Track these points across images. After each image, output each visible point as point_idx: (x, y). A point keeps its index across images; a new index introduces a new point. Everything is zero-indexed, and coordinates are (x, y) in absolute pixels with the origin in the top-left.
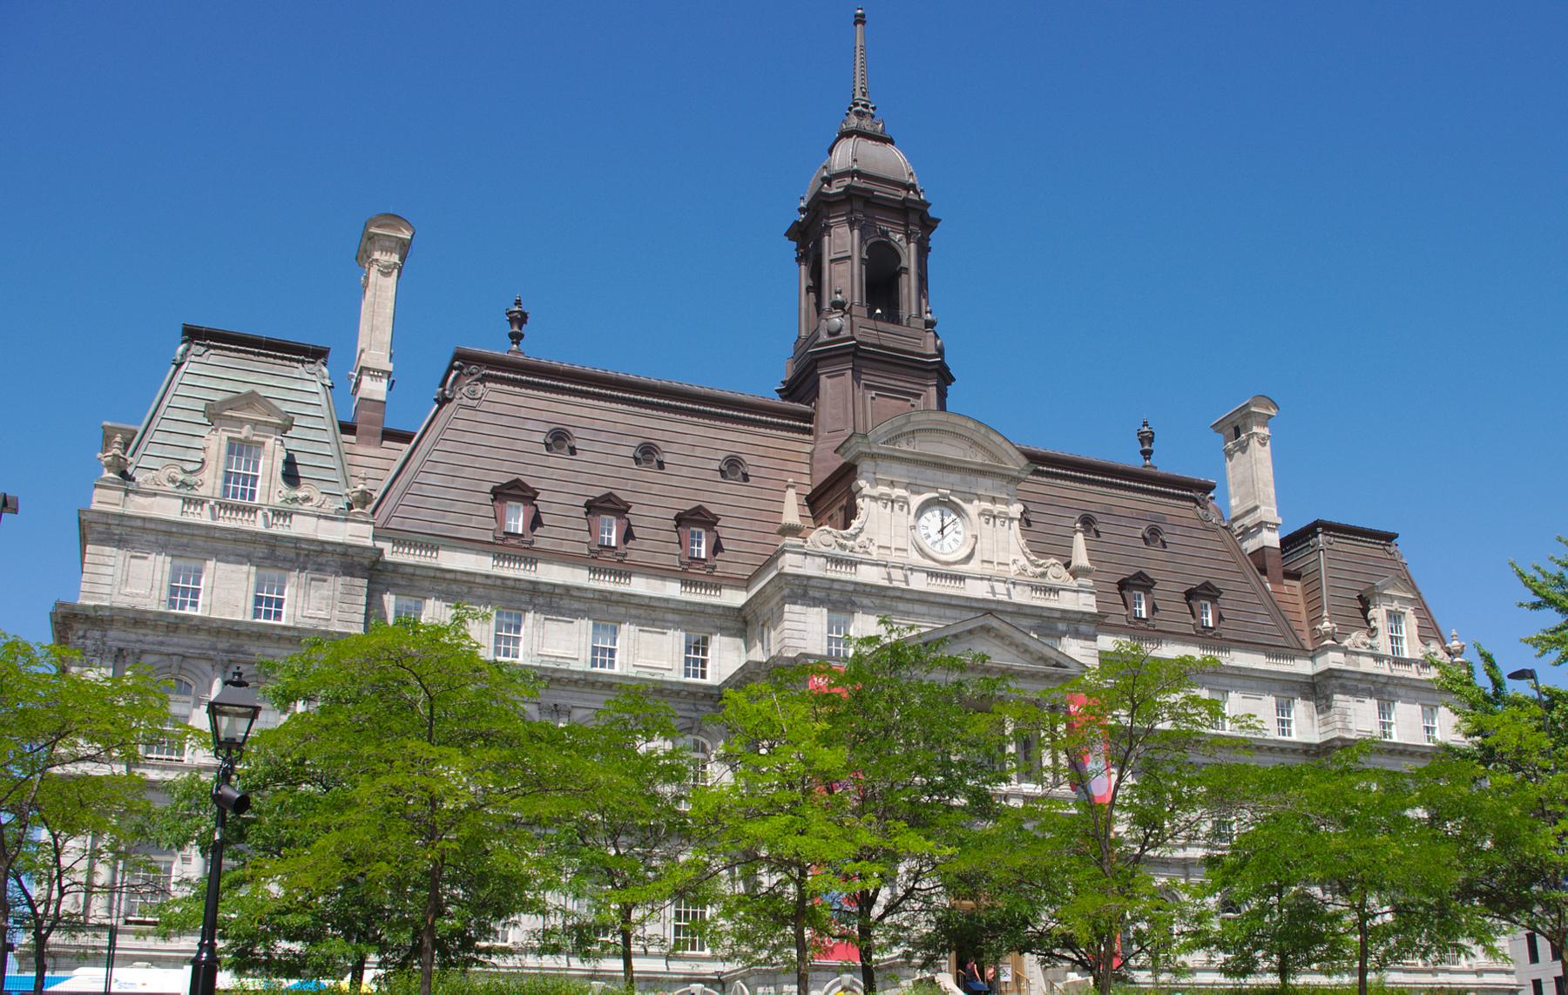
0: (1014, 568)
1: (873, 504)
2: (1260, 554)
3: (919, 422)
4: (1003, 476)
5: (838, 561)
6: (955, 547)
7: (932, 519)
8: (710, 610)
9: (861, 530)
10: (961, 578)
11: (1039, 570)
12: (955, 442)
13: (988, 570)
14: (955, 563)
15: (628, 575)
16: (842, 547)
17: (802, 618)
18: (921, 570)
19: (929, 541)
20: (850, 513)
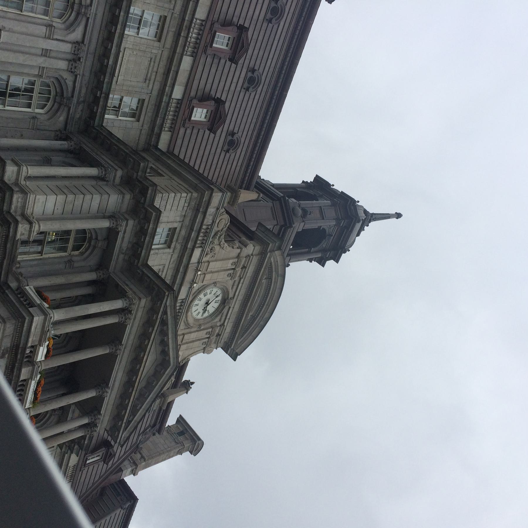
2: (121, 470)
3: (276, 282)
8: (158, 122)
15: (194, 55)
16: (216, 234)
17: (174, 208)
20: (230, 240)
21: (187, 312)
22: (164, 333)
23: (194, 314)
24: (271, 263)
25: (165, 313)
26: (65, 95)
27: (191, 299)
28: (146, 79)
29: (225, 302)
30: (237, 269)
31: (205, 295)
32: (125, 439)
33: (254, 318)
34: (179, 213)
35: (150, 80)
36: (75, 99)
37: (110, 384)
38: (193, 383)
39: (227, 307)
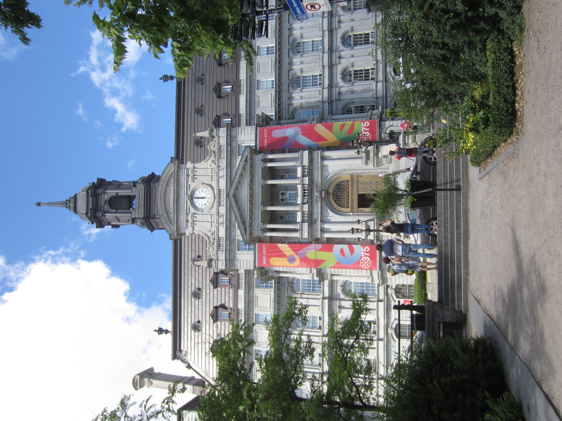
0: (213, 166)
1: (195, 229)
3: (162, 210)
4: (178, 172)
5: (219, 245)
6: (208, 192)
8: (247, 280)
9: (206, 235)
10: (219, 191)
12: (168, 193)
13: (215, 178)
14: (214, 193)
15: (238, 310)
16: (213, 243)
18: (218, 209)
19: (208, 204)
21: (214, 196)
22: (241, 216)
23: (208, 192)
24: (171, 224)
25: (245, 229)
27: (215, 204)
29: (192, 198)
33: (167, 185)
36: (286, 286)
37: (260, 186)
38: (161, 79)
39: (189, 194)
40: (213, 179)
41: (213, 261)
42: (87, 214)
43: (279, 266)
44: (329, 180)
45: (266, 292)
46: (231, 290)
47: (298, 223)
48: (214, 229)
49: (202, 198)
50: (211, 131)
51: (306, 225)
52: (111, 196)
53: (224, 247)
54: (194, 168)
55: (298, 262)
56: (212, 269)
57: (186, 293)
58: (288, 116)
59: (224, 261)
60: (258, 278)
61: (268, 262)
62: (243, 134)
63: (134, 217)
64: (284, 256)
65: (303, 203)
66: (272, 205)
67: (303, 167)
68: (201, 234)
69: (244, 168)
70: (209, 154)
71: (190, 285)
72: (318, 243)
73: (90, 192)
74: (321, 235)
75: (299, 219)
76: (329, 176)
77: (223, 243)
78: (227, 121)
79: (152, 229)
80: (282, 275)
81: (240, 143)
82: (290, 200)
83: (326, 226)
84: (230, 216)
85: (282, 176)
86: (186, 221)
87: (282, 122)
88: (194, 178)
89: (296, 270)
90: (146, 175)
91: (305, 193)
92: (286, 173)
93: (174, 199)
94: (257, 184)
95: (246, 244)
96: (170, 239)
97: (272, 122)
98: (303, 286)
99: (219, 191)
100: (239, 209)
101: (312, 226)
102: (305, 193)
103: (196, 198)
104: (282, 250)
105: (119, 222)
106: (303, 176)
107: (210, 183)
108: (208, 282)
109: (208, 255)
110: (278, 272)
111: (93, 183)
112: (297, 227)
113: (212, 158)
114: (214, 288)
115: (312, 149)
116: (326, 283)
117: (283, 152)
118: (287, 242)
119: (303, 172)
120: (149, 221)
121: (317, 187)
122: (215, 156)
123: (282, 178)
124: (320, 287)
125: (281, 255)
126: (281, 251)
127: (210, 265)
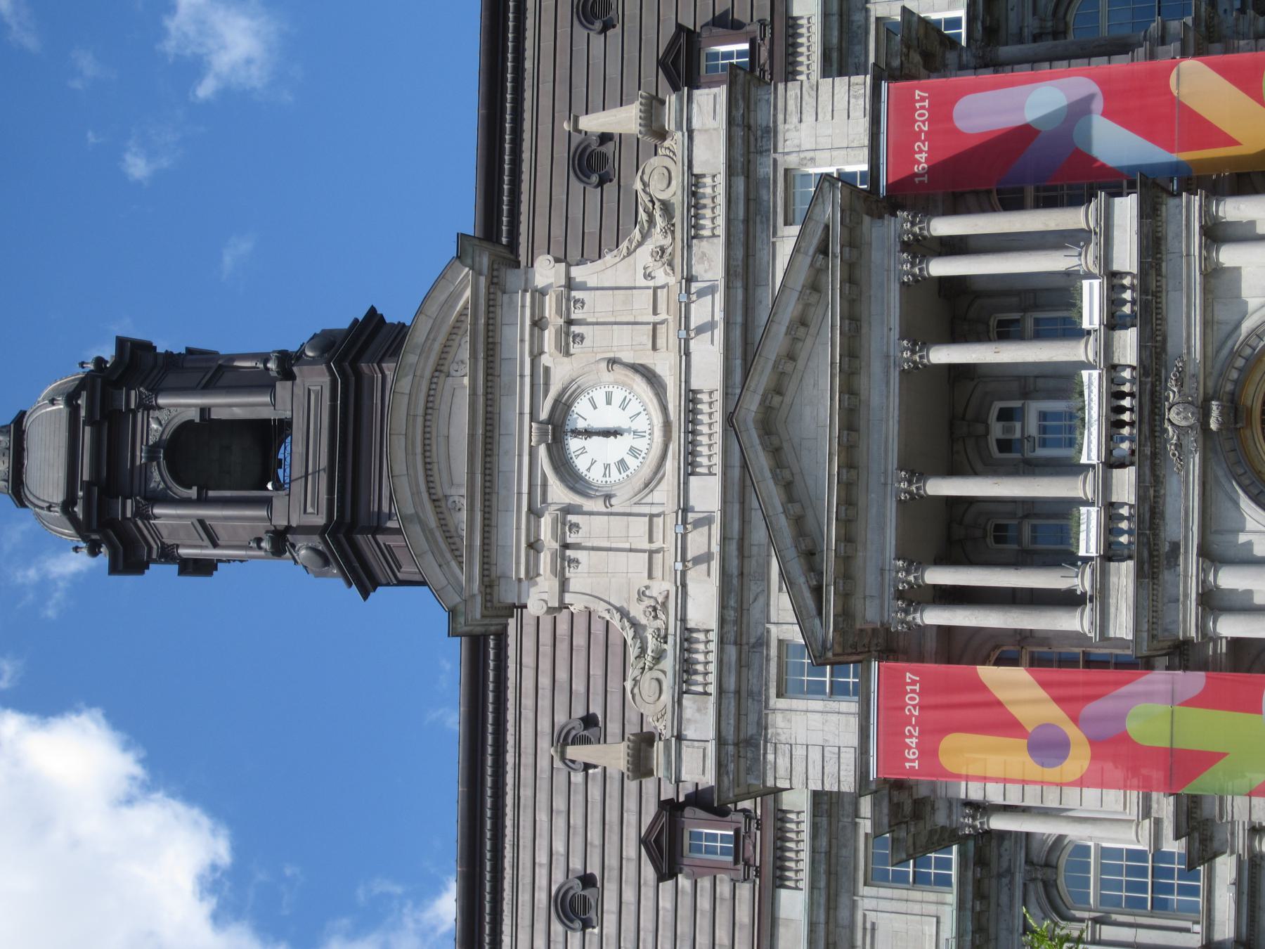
0: (662, 276)
1: (574, 585)
3: (415, 494)
4: (491, 305)
5: (686, 668)
6: (634, 407)
7: (590, 457)
8: (824, 842)
9: (624, 614)
10: (691, 398)
11: (660, 221)
12: (444, 408)
13: (669, 336)
17: (799, 752)
19: (632, 463)
21: (667, 425)
22: (798, 523)
24: (458, 557)
25: (818, 591)
26: (1040, 885)
27: (670, 465)
28: (873, 929)
30: (556, 546)
31: (622, 464)
32: (820, 200)
34: (783, 738)
35: (865, 929)
36: (1019, 879)
40: (661, 342)
41: (659, 747)
42: (67, 506)
43: (985, 779)
44: (1246, 343)
45: (916, 908)
46: (744, 891)
47: (1086, 560)
48: (663, 586)
49: (607, 433)
50: (653, 107)
51: (1123, 575)
52: (177, 422)
53: (712, 678)
54: (570, 284)
55: (1078, 761)
56: (649, 784)
57: (524, 897)
58: (1031, 24)
59: (711, 748)
60: (877, 834)
61: (929, 753)
62: (809, 117)
63: (281, 522)
64: (1008, 726)
65: (1112, 463)
66: (953, 470)
67: (1113, 278)
68: (600, 609)
69: (815, 286)
70: (643, 216)
71: (542, 858)
72: (1186, 668)
73: (81, 402)
74: (1201, 627)
75: (1088, 542)
76: (1246, 326)
77: (707, 655)
78: (728, 55)
79: (365, 579)
80: (998, 823)
81: (792, 161)
82: (1044, 444)
83: (1229, 579)
84: (744, 521)
85: (1001, 323)
86: (530, 546)
87: (1005, 51)
88: (568, 337)
89: (1072, 797)
90: (342, 321)
91: (1122, 410)
92: (1025, 310)
93: (472, 436)
94: (876, 366)
95: (819, 661)
96: (452, 633)
97: (951, 57)
98: (1104, 884)
99: (691, 398)
100: (788, 487)
101: (1154, 576)
102: (1122, 410)
103: (577, 433)
104: (1001, 695)
105: (215, 545)
106: (1114, 322)
107: (647, 359)
108: (631, 849)
109: (632, 717)
110: (981, 808)
111: (99, 361)
112: (1082, 582)
113: (658, 238)
114: (661, 878)
115: (1155, 184)
116: (1226, 868)
117: (1012, 202)
118: (1025, 658)
119: (1112, 303)
120: (354, 545)
121: (1180, 383)
122: (670, 229)
123: (1006, 333)
124: (1194, 891)
125: (997, 721)
126: (999, 704)
127: (640, 766)
